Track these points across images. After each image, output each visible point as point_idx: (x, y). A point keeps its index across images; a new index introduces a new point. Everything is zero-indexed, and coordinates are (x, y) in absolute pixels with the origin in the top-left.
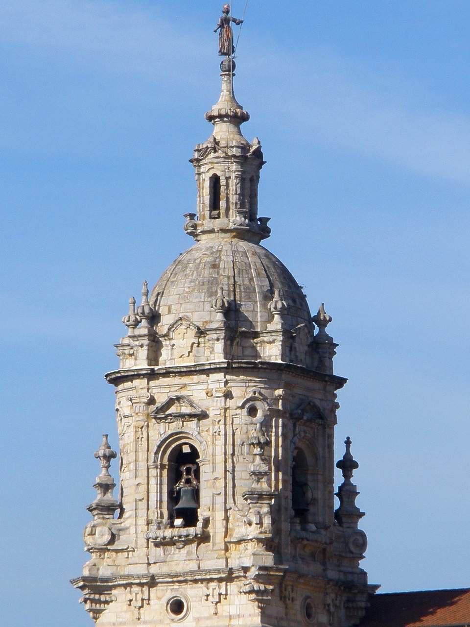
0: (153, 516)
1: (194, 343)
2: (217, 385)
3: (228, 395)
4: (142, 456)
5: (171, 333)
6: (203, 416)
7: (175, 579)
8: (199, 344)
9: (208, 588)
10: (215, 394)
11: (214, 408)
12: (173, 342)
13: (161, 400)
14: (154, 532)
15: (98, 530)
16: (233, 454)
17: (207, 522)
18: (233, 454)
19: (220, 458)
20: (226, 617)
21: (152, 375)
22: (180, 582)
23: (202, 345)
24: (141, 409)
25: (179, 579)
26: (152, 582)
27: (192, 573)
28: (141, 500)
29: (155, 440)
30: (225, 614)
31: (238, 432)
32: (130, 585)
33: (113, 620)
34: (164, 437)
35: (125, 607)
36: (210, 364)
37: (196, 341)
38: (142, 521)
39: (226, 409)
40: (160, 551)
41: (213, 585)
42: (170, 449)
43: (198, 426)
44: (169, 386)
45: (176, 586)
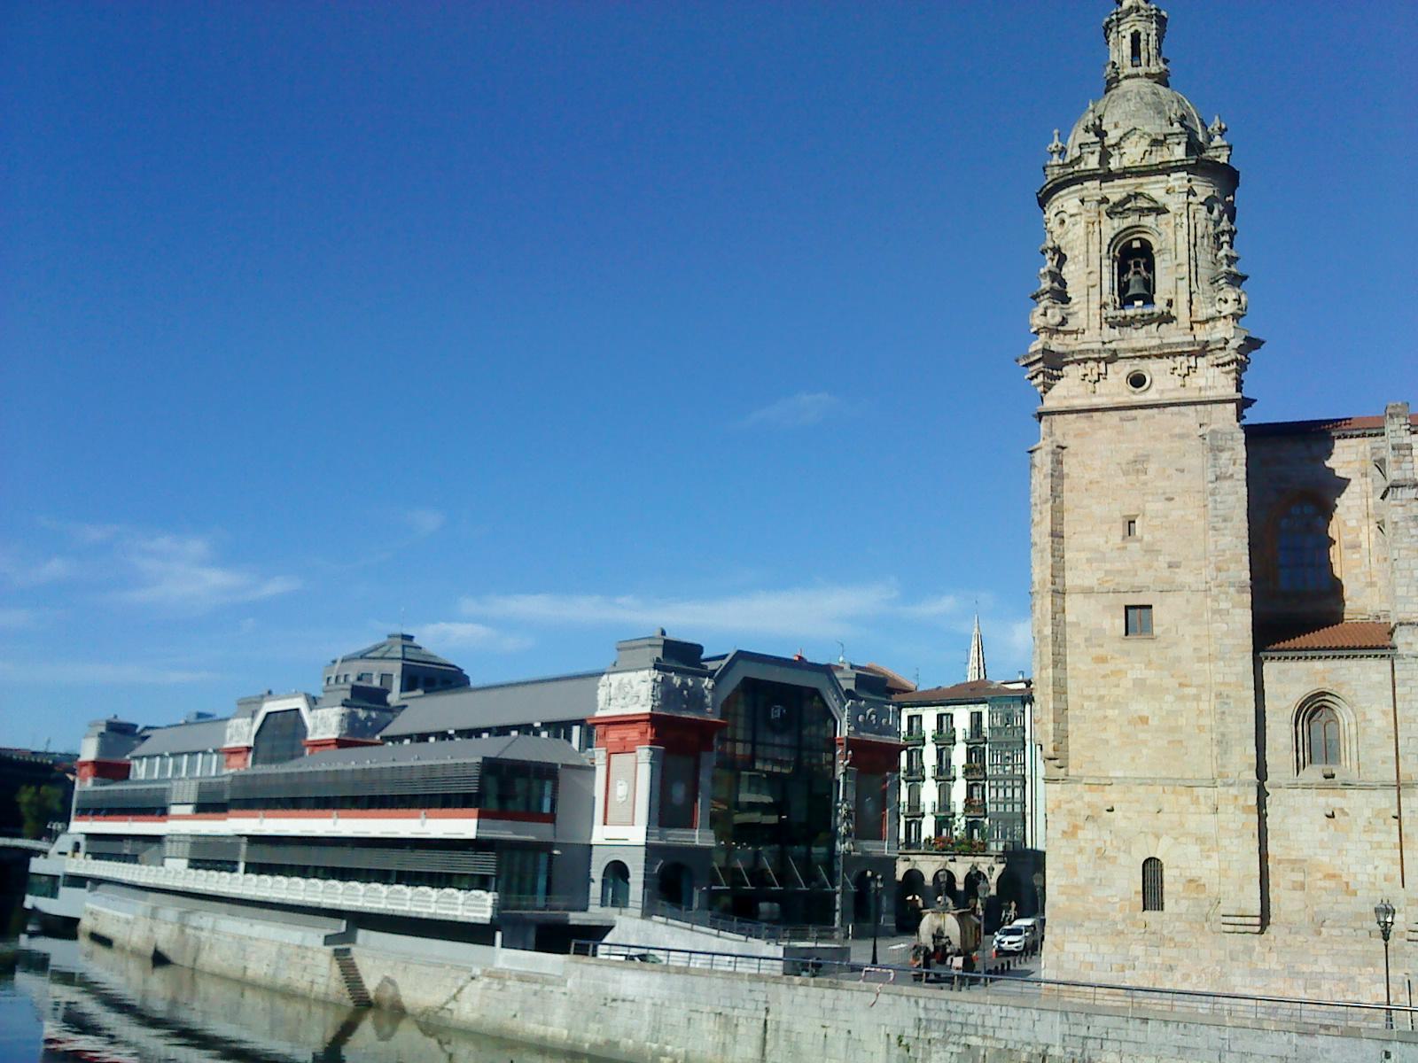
0: (1107, 298)
1: (1147, 151)
2: (1179, 182)
3: (1191, 192)
4: (1094, 248)
5: (1122, 143)
6: (1161, 210)
7: (1138, 354)
8: (1151, 151)
9: (1174, 362)
10: (1177, 189)
11: (1175, 203)
12: (1122, 151)
13: (1114, 198)
14: (1110, 312)
15: (1049, 312)
16: (1195, 245)
17: (1170, 303)
18: (1195, 245)
19: (1183, 247)
20: (1195, 388)
21: (1108, 176)
22: (1142, 357)
23: (1154, 153)
24: (1093, 207)
25: (1142, 355)
26: (1113, 358)
27: (1159, 347)
28: (1093, 286)
29: (1108, 234)
30: (1194, 385)
31: (1198, 226)
32: (1085, 361)
33: (1065, 393)
34: (1117, 231)
35: (1078, 381)
36: (1176, 161)
37: (1149, 149)
38: (1095, 306)
39: (1189, 204)
40: (1116, 332)
41: (1179, 359)
42: (1125, 241)
43: (1156, 220)
44: (1123, 186)
45: (1137, 361)
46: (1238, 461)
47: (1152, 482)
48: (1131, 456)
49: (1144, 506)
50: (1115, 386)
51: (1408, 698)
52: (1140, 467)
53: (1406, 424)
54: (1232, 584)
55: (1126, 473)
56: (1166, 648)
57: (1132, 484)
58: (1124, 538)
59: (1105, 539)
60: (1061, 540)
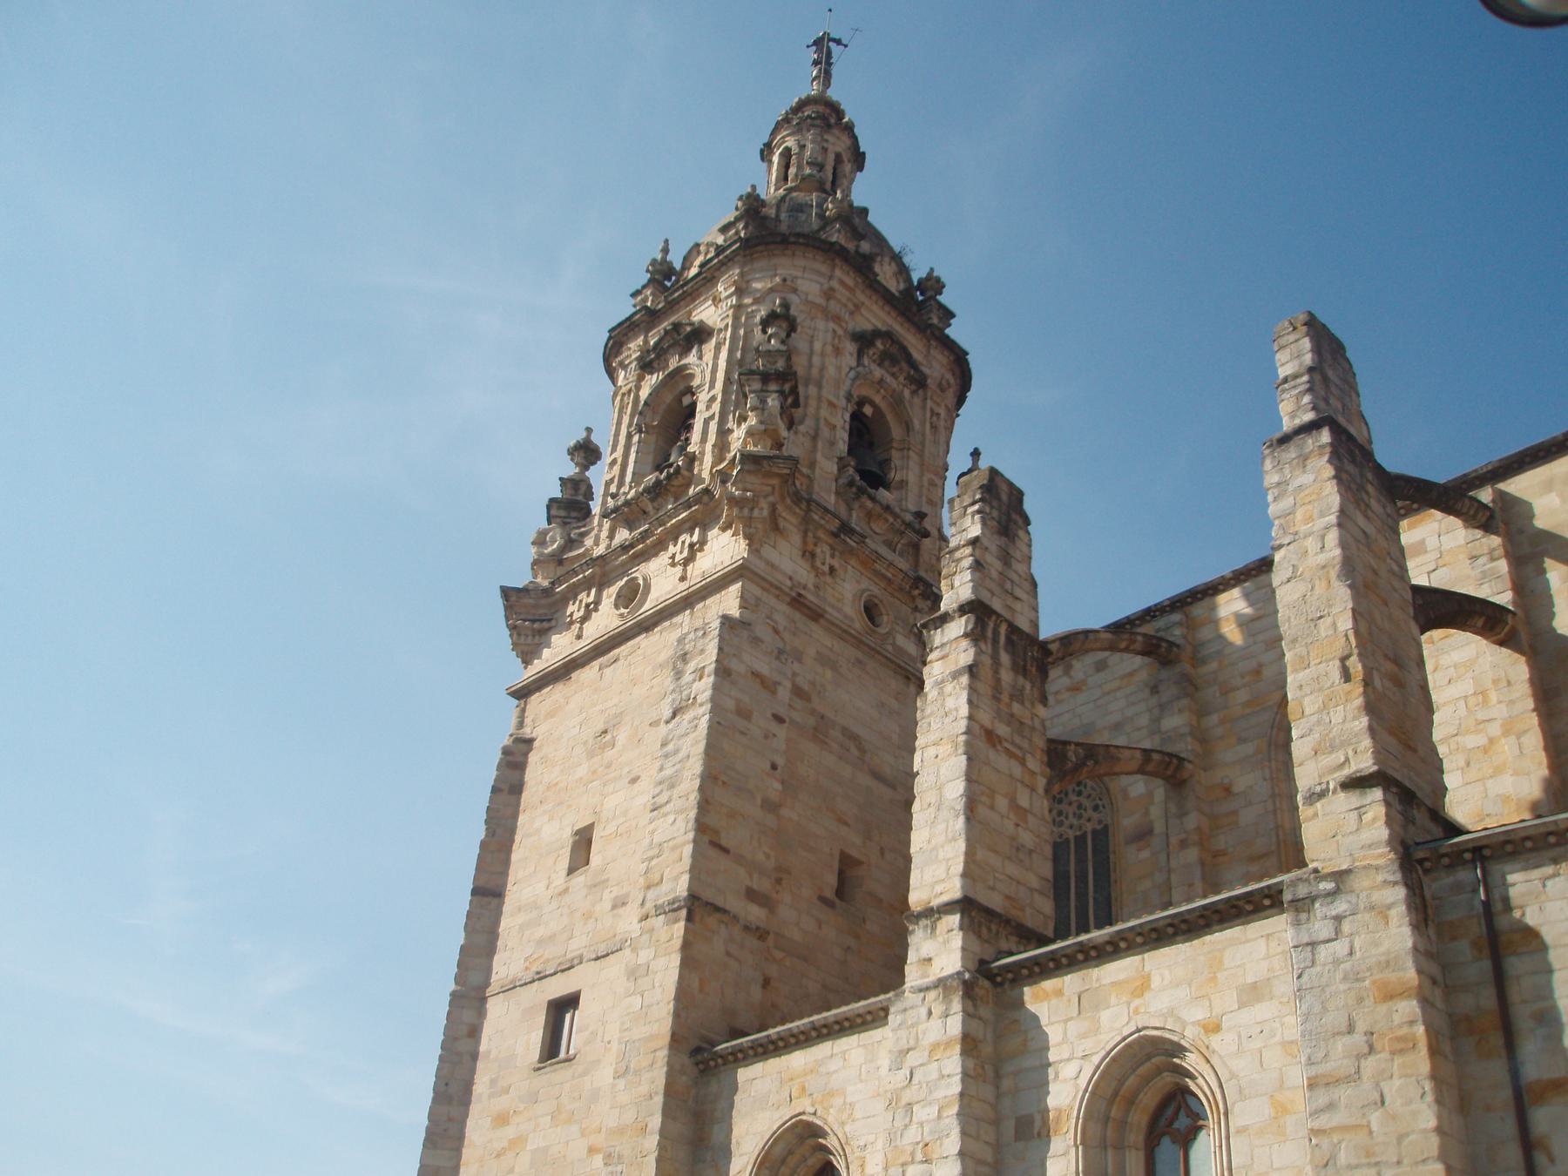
46: (706, 671)
47: (617, 760)
48: (600, 727)
49: (602, 805)
50: (607, 619)
51: (907, 1097)
52: (608, 737)
53: (973, 504)
54: (660, 910)
55: (591, 754)
56: (585, 1073)
57: (594, 772)
58: (571, 870)
59: (546, 882)
60: (495, 901)
